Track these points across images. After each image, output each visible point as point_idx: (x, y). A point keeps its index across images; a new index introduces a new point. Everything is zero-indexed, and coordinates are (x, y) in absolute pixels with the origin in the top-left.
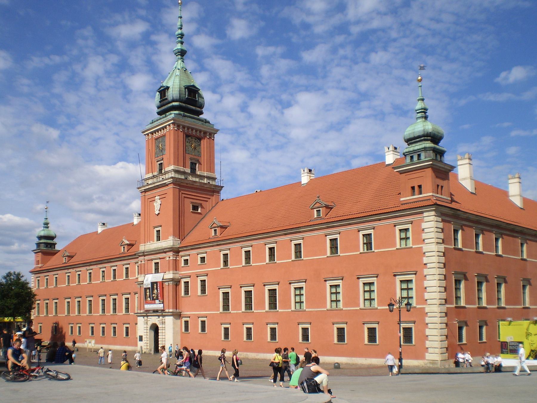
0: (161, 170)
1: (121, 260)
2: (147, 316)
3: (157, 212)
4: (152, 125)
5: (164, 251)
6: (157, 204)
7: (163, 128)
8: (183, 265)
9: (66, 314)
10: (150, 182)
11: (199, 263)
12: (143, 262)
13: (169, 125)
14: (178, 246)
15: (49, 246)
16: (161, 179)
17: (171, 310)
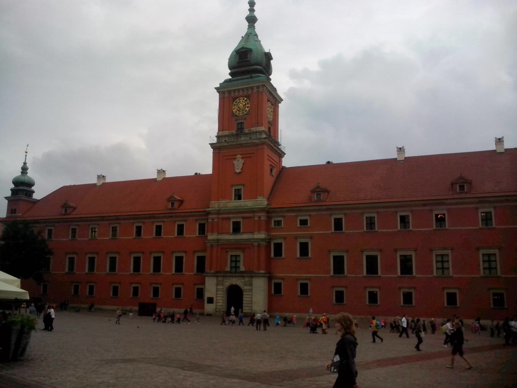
0: (240, 128)
1: (171, 217)
2: (223, 276)
3: (238, 171)
4: (229, 84)
5: (252, 211)
6: (238, 164)
7: (247, 89)
8: (273, 225)
9: (67, 270)
10: (227, 139)
11: (299, 225)
12: (216, 220)
13: (258, 87)
14: (269, 207)
15: (28, 194)
16: (248, 138)
17: (262, 272)
